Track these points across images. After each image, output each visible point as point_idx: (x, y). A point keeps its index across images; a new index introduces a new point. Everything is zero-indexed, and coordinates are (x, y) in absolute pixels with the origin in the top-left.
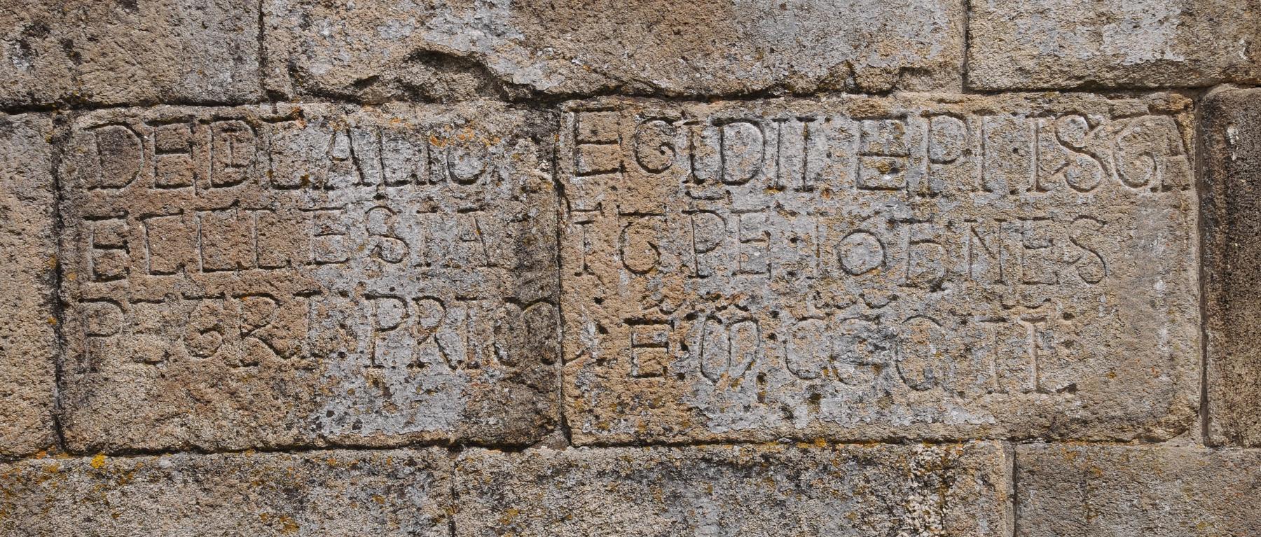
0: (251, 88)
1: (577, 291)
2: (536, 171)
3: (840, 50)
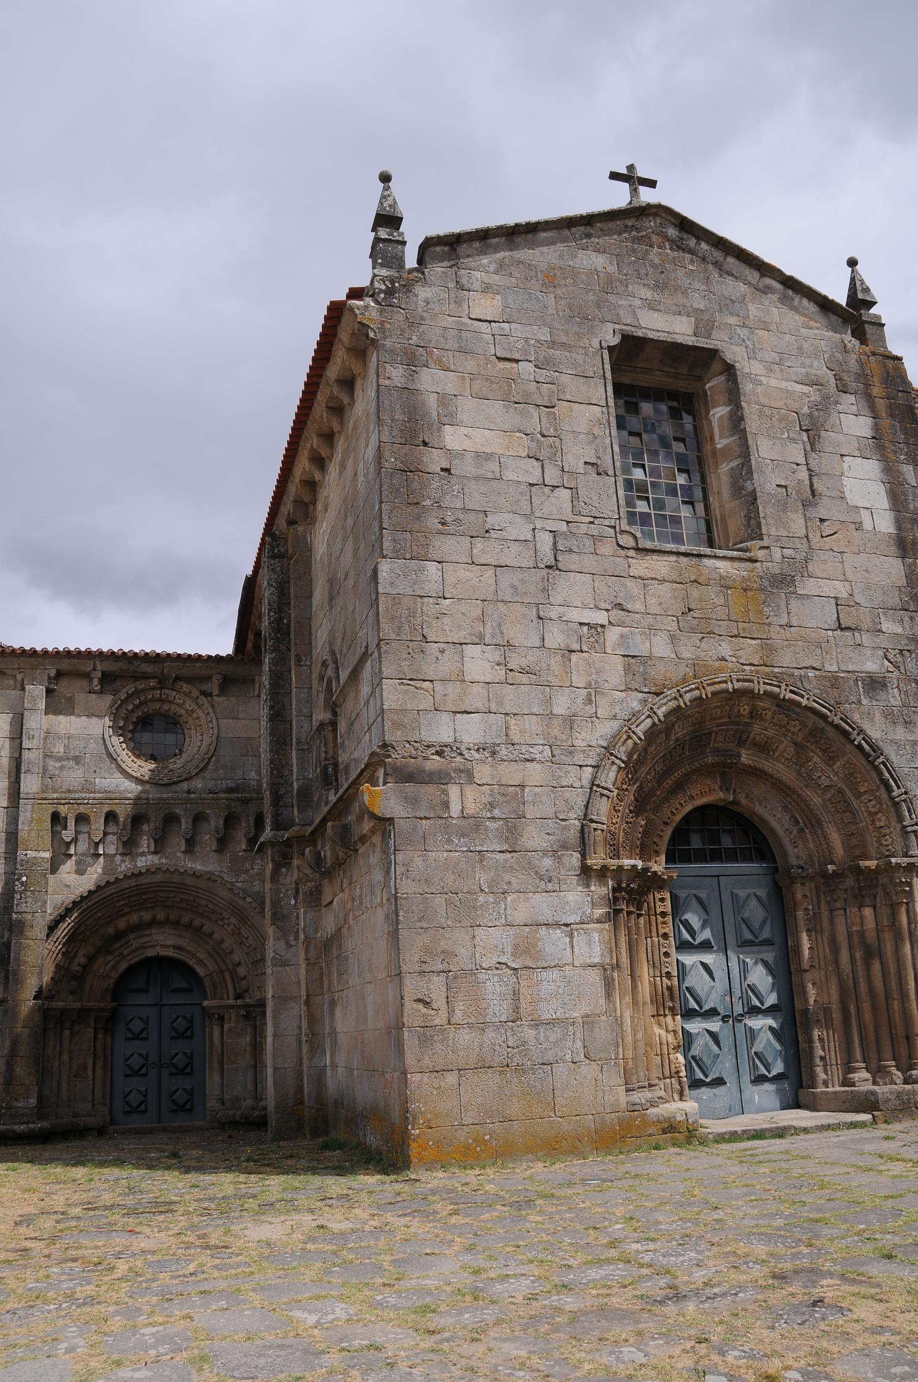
2: (515, 980)
3: (556, 961)
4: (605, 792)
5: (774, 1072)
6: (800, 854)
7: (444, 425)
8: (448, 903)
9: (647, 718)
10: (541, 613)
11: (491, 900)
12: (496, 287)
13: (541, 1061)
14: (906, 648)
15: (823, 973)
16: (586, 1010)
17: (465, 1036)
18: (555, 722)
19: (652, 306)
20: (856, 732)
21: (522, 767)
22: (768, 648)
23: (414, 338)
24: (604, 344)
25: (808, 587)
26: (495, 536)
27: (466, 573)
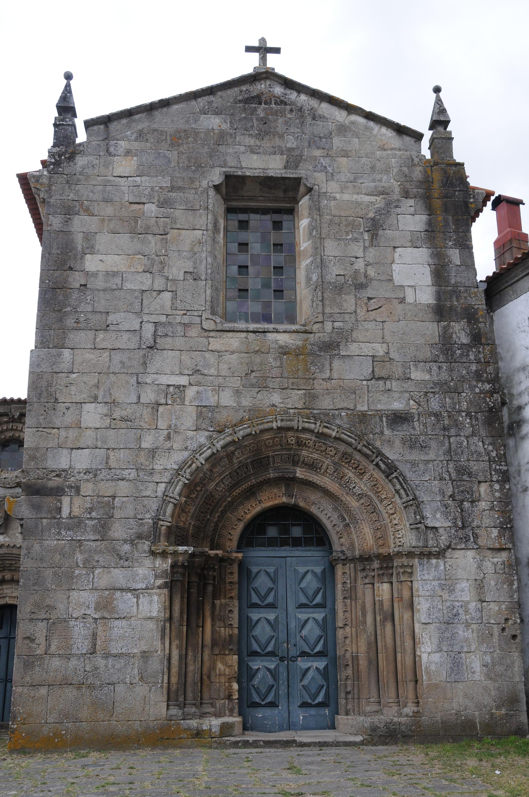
0: (67, 617)
1: (98, 638)
2: (95, 626)
4: (172, 500)
5: (316, 702)
6: (345, 543)
7: (86, 254)
8: (55, 574)
9: (208, 449)
10: (140, 380)
11: (84, 572)
12: (134, 151)
13: (107, 682)
14: (430, 390)
15: (354, 630)
16: (145, 648)
17: (56, 662)
18: (142, 453)
19: (253, 151)
20: (375, 455)
21: (115, 484)
22: (311, 396)
23: (72, 195)
24: (211, 184)
25: (353, 349)
26: (114, 329)
27: (89, 356)
